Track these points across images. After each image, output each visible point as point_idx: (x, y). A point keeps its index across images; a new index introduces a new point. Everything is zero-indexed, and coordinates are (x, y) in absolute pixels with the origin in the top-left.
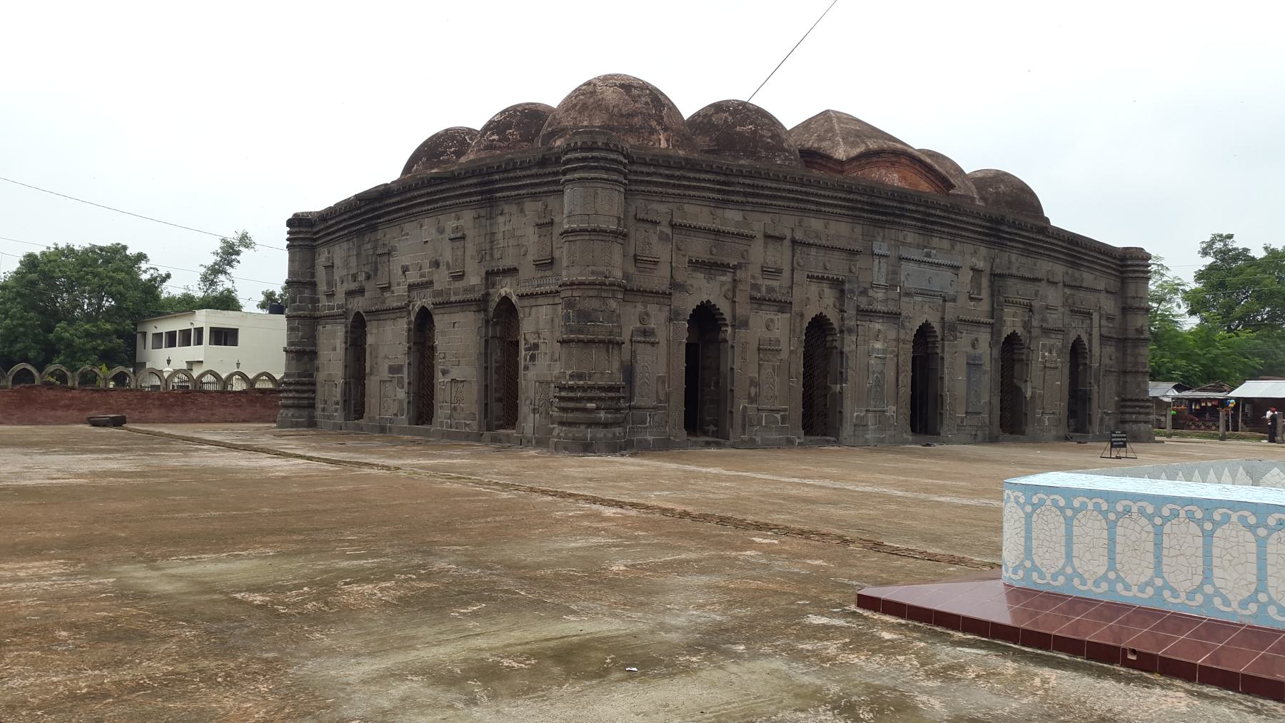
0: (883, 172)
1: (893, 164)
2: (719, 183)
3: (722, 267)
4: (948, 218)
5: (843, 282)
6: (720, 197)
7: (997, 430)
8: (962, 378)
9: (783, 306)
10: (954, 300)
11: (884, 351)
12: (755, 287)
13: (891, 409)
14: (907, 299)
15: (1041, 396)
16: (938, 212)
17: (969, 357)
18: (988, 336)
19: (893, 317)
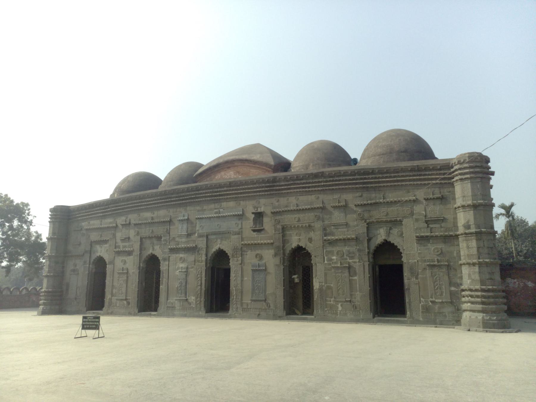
0: (223, 173)
1: (229, 168)
2: (103, 209)
3: (105, 242)
4: (230, 190)
5: (161, 237)
6: (101, 214)
7: (281, 311)
8: (248, 279)
9: (129, 253)
10: (239, 234)
11: (187, 268)
12: (119, 247)
13: (192, 299)
14: (201, 239)
15: (329, 288)
16: (225, 189)
17: (253, 266)
18: (272, 252)
19: (193, 250)
